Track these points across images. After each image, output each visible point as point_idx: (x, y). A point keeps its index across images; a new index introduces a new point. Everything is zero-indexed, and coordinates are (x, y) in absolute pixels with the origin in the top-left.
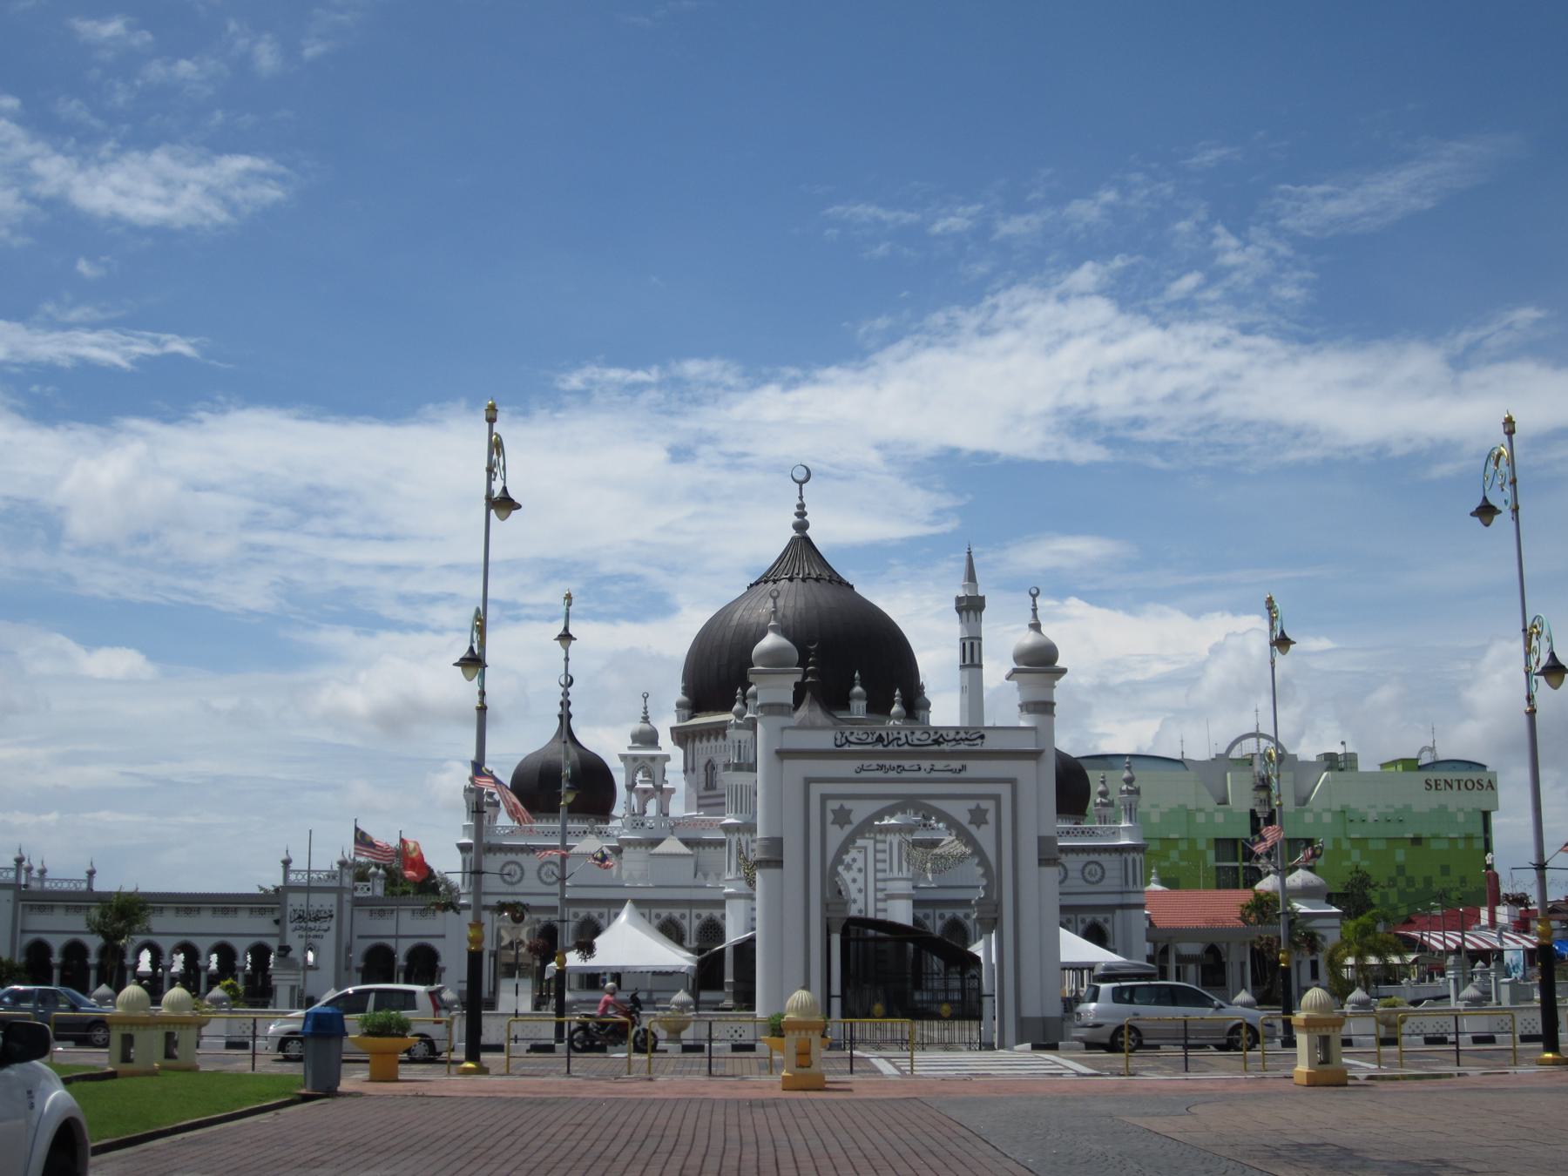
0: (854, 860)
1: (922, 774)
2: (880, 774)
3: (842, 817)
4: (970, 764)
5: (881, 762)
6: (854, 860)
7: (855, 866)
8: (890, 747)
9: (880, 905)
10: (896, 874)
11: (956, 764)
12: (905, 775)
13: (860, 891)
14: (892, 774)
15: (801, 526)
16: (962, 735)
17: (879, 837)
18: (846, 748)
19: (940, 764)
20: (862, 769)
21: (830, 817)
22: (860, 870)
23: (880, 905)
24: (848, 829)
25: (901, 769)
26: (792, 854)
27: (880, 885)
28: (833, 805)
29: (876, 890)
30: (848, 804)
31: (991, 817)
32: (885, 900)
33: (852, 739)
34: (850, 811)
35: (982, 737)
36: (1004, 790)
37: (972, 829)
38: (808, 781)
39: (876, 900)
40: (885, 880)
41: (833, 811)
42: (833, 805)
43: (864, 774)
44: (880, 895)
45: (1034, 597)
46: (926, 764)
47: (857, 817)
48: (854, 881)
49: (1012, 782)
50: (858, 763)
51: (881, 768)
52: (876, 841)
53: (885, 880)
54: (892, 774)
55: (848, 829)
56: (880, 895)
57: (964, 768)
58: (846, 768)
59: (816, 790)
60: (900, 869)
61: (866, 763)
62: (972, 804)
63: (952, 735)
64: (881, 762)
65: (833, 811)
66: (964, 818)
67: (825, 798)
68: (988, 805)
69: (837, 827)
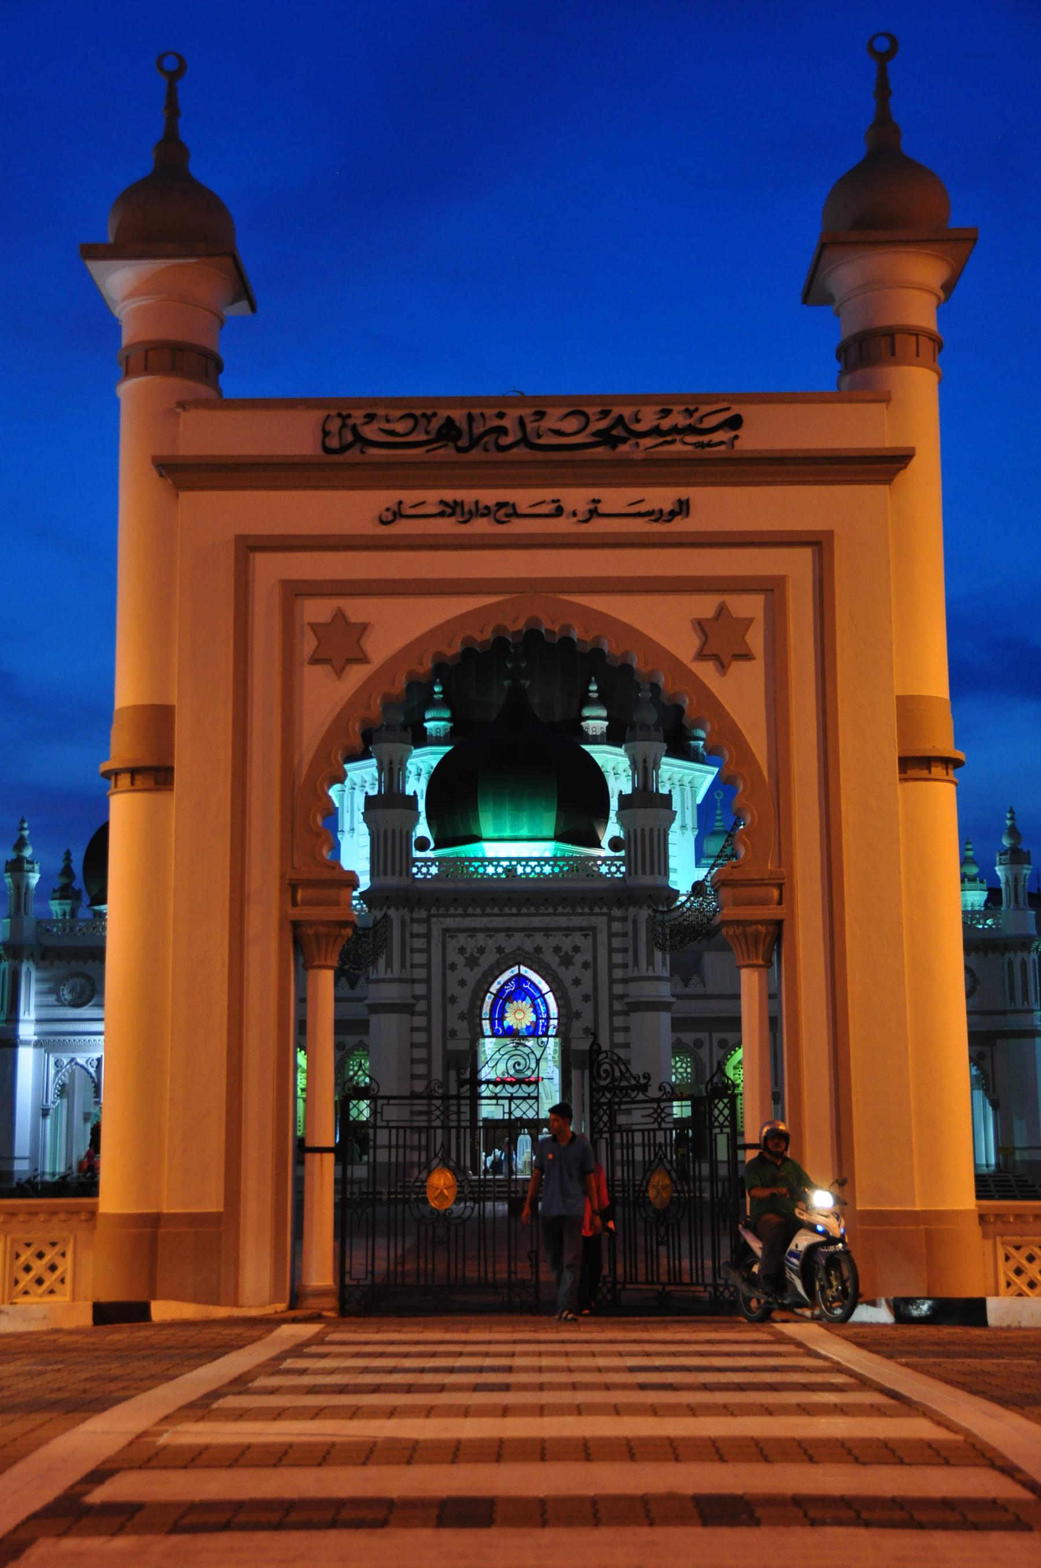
0: (576, 949)
1: (563, 525)
2: (447, 526)
3: (341, 645)
4: (699, 495)
5: (450, 495)
6: (576, 949)
7: (579, 959)
8: (476, 454)
9: (619, 1021)
10: (644, 971)
11: (663, 497)
12: (519, 527)
13: (586, 998)
16: (678, 419)
17: (616, 912)
18: (353, 455)
19: (615, 498)
20: (397, 514)
21: (308, 644)
22: (585, 965)
23: (619, 1021)
24: (357, 675)
25: (509, 511)
26: (200, 754)
27: (618, 989)
28: (316, 610)
29: (613, 997)
30: (357, 609)
31: (756, 640)
32: (626, 1013)
33: (370, 432)
34: (364, 628)
35: (735, 423)
36: (796, 566)
37: (706, 672)
38: (249, 546)
39: (613, 1013)
40: (625, 981)
42: (316, 610)
43: (403, 527)
44: (618, 1006)
45: (883, 58)
47: (381, 647)
48: (577, 982)
49: (819, 544)
50: (386, 498)
51: (451, 509)
52: (611, 919)
53: (625, 981)
54: (481, 526)
55: (357, 675)
56: (618, 1006)
57: (683, 508)
58: (354, 509)
59: (270, 570)
60: (650, 962)
61: (410, 496)
62: (705, 606)
63: (649, 419)
67: (294, 591)
68: (749, 606)
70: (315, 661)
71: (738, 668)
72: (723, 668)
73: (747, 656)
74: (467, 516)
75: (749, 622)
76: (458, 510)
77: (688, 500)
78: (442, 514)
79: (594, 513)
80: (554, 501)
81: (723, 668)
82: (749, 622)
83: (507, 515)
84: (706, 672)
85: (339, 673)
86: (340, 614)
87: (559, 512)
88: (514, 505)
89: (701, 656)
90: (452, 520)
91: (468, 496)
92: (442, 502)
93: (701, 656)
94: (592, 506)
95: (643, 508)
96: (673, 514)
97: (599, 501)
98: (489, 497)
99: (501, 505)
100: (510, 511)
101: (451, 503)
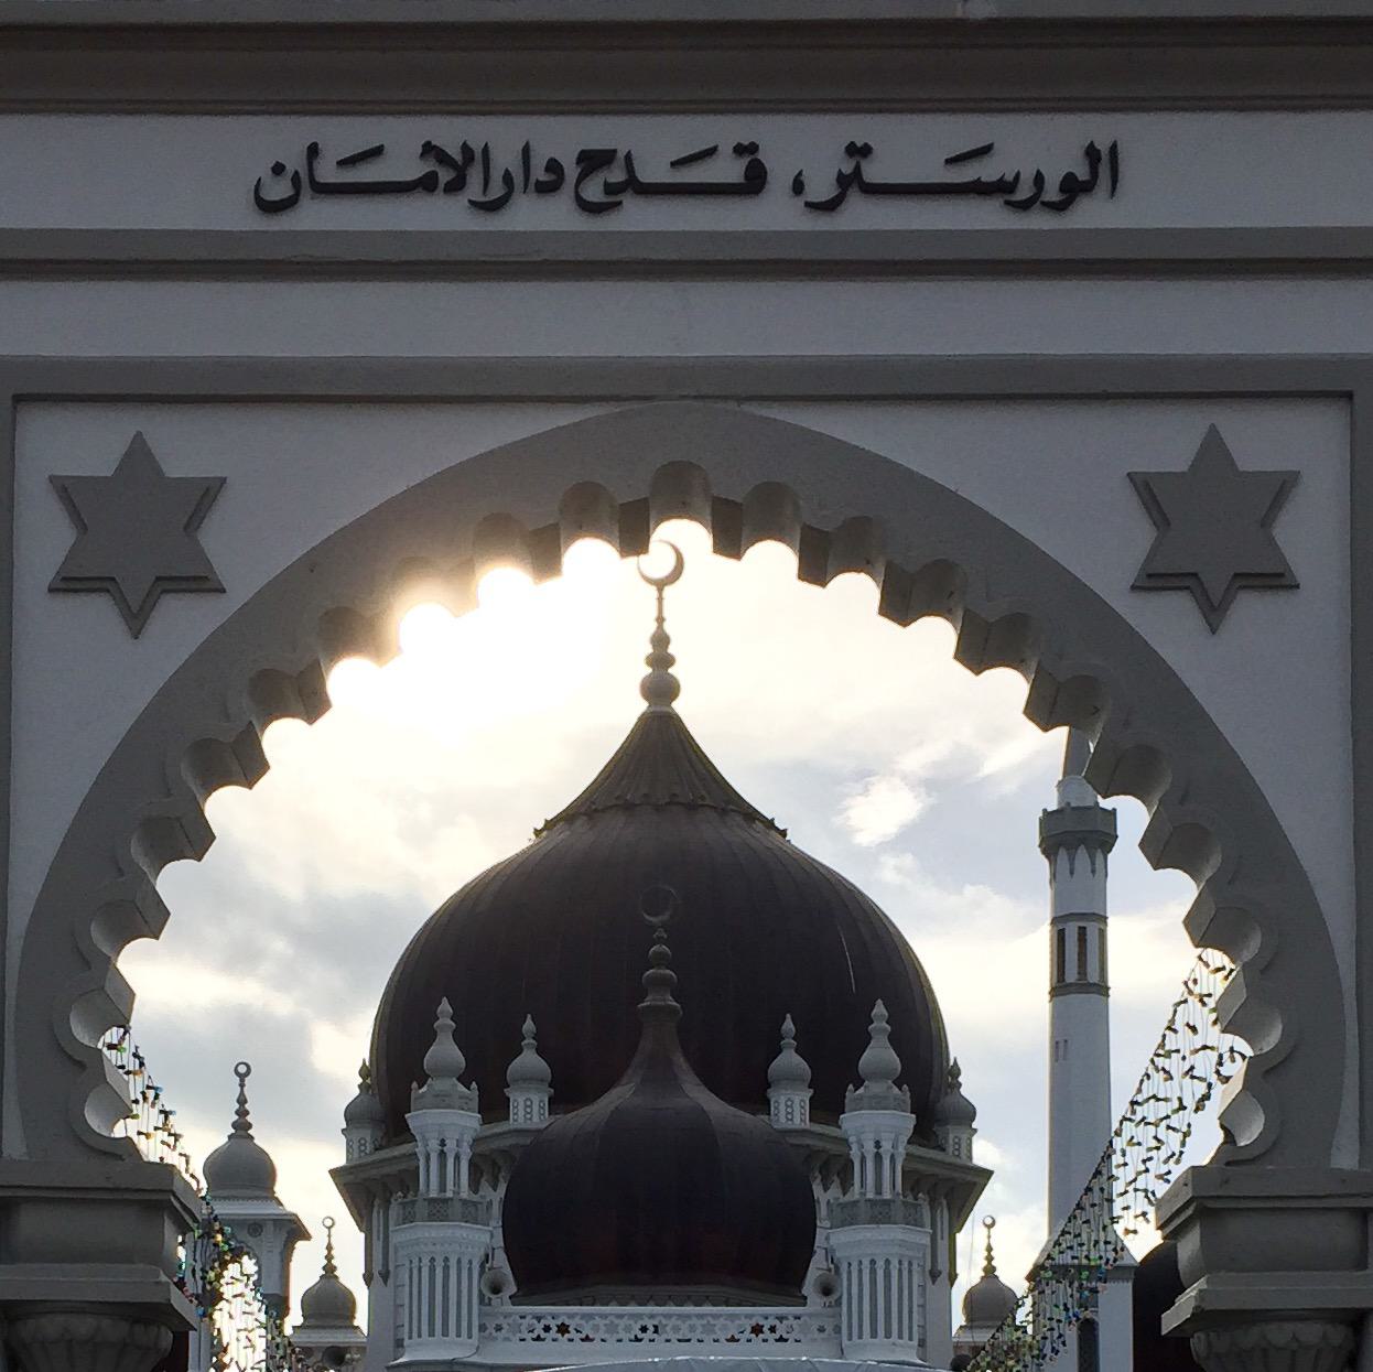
2: (444, 216)
5: (451, 133)
14: (541, 218)
15: (661, 688)
19: (912, 145)
34: (207, 493)
37: (1168, 626)
41: (67, 491)
46: (805, 145)
51: (449, 171)
54: (541, 218)
55: (184, 626)
61: (341, 135)
62: (1167, 441)
64: (451, 133)
65: (67, 491)
66: (1102, 550)
69: (98, 611)
70: (68, 583)
71: (1249, 609)
72: (1213, 613)
73: (1277, 580)
74: (497, 191)
75: (1282, 487)
76: (475, 176)
77: (1114, 149)
78: (427, 184)
79: (850, 182)
80: (740, 150)
81: (1213, 613)
82: (1282, 487)
83: (610, 189)
84: (1168, 626)
85: (136, 619)
86: (138, 455)
87: (755, 181)
88: (628, 157)
89: (1153, 581)
90: (461, 201)
91: (503, 137)
92: (429, 149)
93: (1153, 581)
94: (848, 169)
95: (987, 171)
96: (1073, 189)
97: (866, 151)
98: (561, 138)
99: (593, 161)
100: (617, 175)
101: (455, 152)
